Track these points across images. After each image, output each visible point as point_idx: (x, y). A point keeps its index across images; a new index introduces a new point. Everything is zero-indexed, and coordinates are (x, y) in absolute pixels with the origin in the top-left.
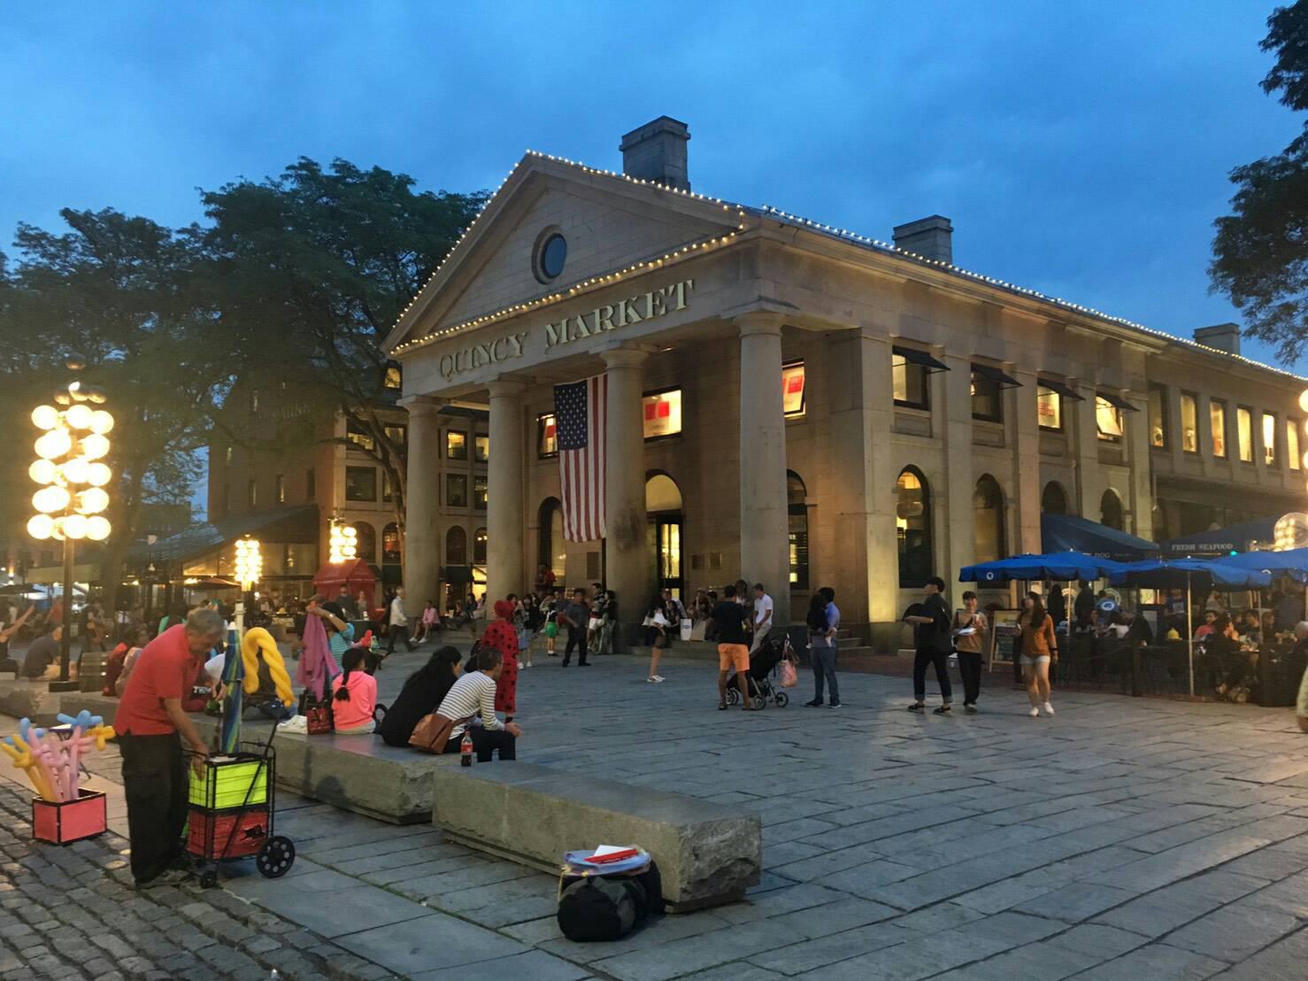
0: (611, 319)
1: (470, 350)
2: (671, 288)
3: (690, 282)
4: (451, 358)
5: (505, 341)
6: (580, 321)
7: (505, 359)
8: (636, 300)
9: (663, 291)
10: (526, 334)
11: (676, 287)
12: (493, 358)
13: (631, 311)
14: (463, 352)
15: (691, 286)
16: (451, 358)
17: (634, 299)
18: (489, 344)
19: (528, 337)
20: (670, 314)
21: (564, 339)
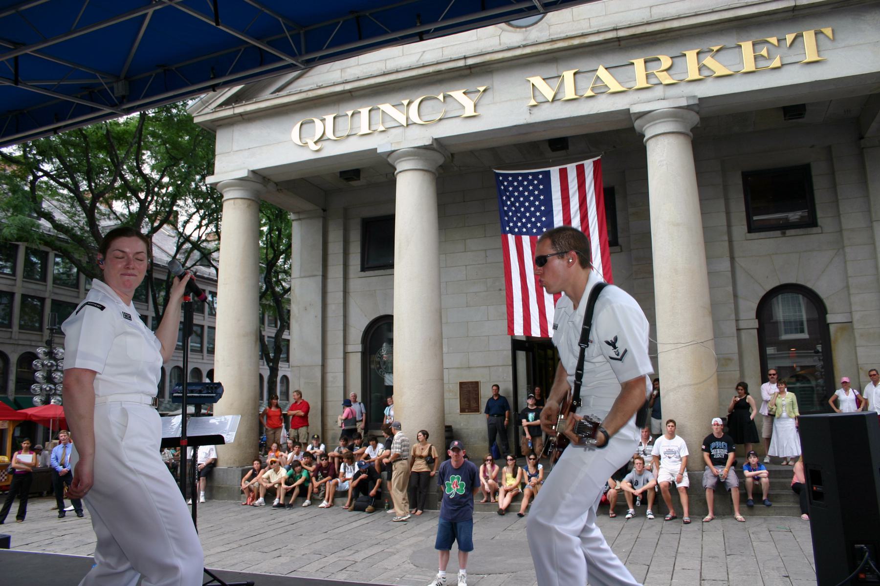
0: (667, 70)
1: (364, 111)
2: (790, 38)
3: (828, 31)
4: (323, 120)
5: (441, 97)
6: (602, 72)
7: (440, 120)
8: (718, 51)
9: (774, 40)
10: (485, 91)
11: (799, 36)
12: (414, 117)
13: (708, 61)
14: (350, 113)
15: (831, 36)
16: (323, 120)
17: (715, 49)
18: (405, 102)
19: (487, 93)
20: (785, 68)
21: (569, 93)
